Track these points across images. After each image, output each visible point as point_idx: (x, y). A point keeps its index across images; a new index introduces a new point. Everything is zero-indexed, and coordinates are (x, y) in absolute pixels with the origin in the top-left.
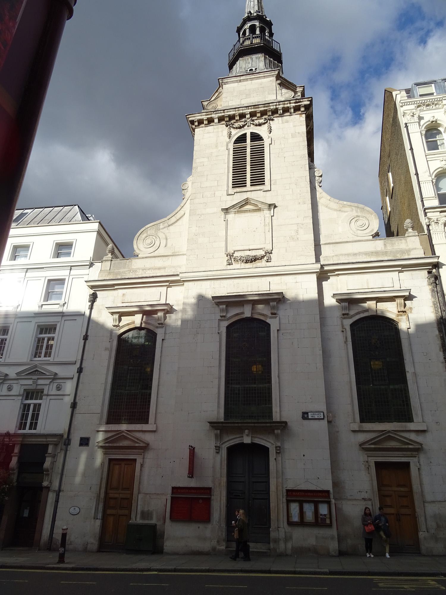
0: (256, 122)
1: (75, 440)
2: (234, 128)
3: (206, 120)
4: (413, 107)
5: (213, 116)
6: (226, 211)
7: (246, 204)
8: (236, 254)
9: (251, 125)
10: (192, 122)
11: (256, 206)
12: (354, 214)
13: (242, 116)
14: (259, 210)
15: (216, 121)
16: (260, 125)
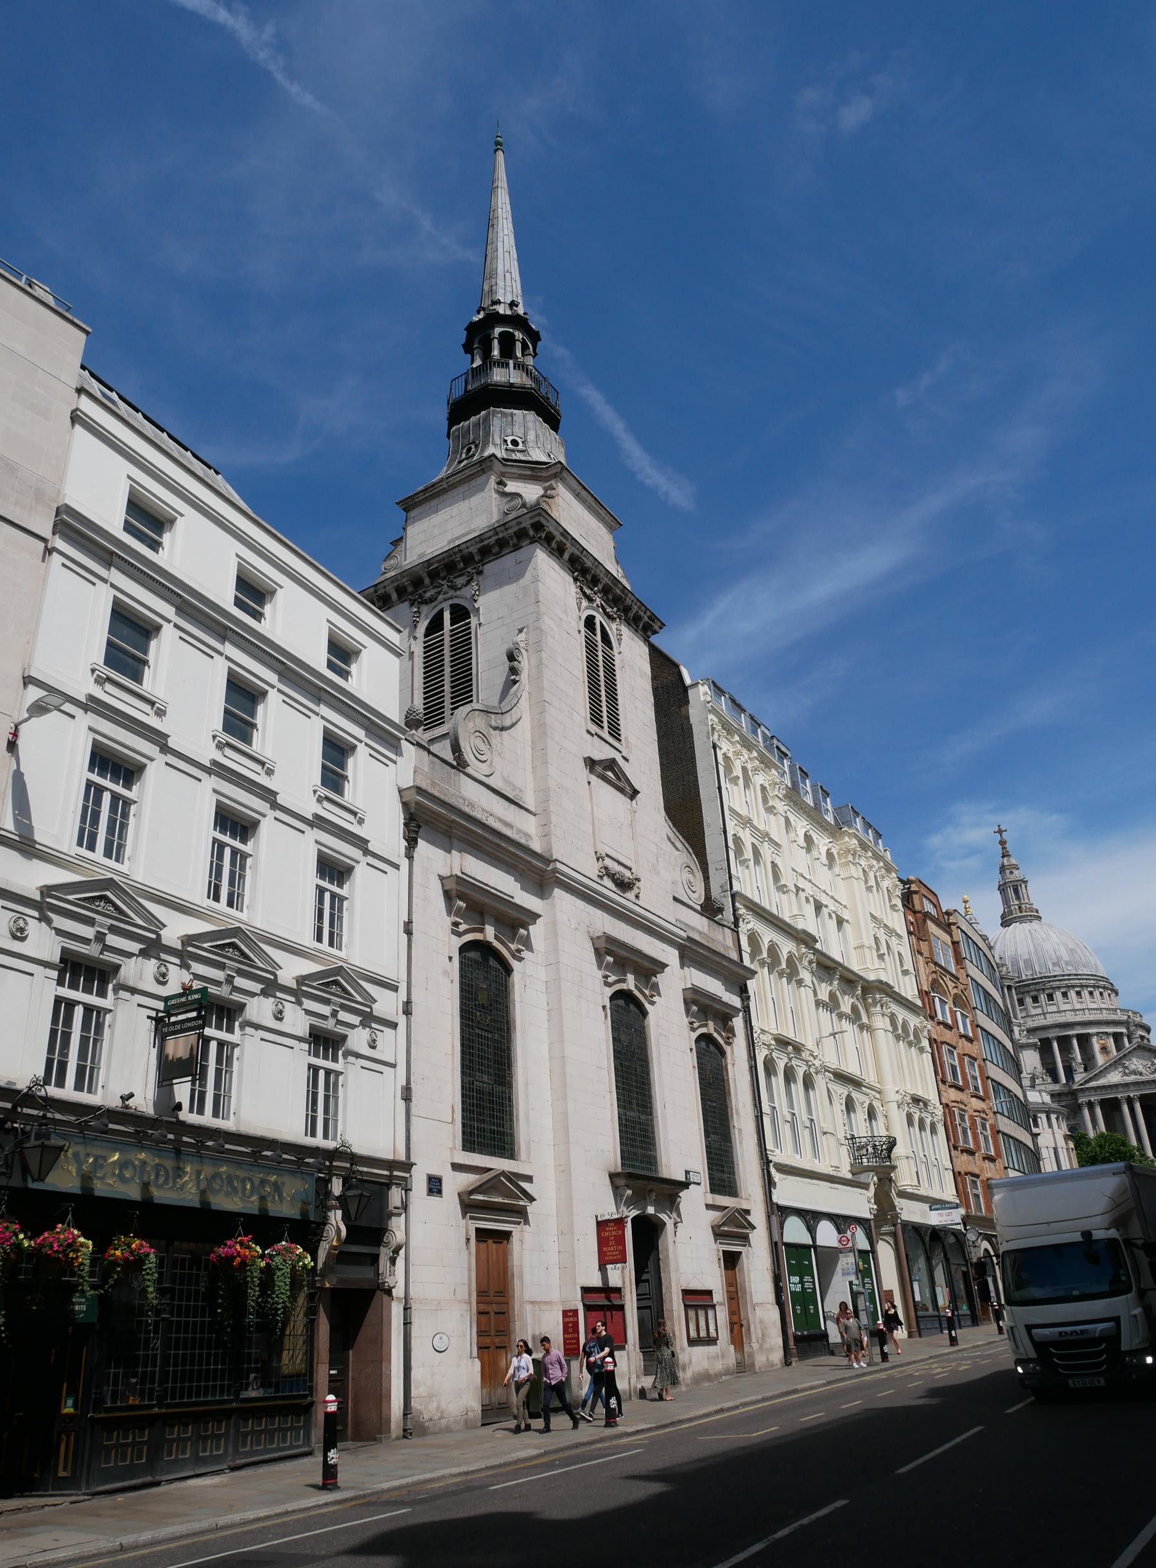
0: (609, 610)
1: (419, 1184)
2: (584, 594)
3: (557, 542)
4: (716, 720)
5: (568, 545)
6: (591, 763)
7: (606, 768)
8: (608, 862)
9: (600, 609)
10: (538, 526)
11: (618, 778)
12: (686, 860)
13: (595, 581)
14: (621, 790)
15: (566, 556)
16: (610, 617)
